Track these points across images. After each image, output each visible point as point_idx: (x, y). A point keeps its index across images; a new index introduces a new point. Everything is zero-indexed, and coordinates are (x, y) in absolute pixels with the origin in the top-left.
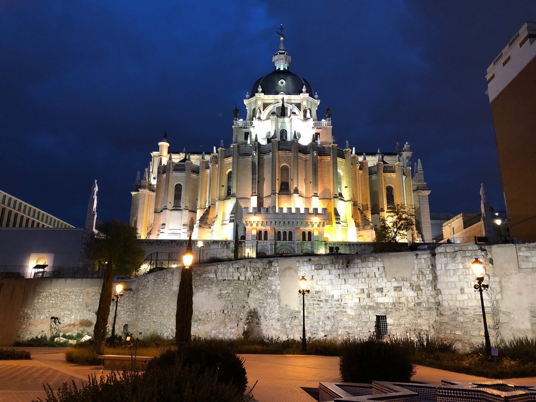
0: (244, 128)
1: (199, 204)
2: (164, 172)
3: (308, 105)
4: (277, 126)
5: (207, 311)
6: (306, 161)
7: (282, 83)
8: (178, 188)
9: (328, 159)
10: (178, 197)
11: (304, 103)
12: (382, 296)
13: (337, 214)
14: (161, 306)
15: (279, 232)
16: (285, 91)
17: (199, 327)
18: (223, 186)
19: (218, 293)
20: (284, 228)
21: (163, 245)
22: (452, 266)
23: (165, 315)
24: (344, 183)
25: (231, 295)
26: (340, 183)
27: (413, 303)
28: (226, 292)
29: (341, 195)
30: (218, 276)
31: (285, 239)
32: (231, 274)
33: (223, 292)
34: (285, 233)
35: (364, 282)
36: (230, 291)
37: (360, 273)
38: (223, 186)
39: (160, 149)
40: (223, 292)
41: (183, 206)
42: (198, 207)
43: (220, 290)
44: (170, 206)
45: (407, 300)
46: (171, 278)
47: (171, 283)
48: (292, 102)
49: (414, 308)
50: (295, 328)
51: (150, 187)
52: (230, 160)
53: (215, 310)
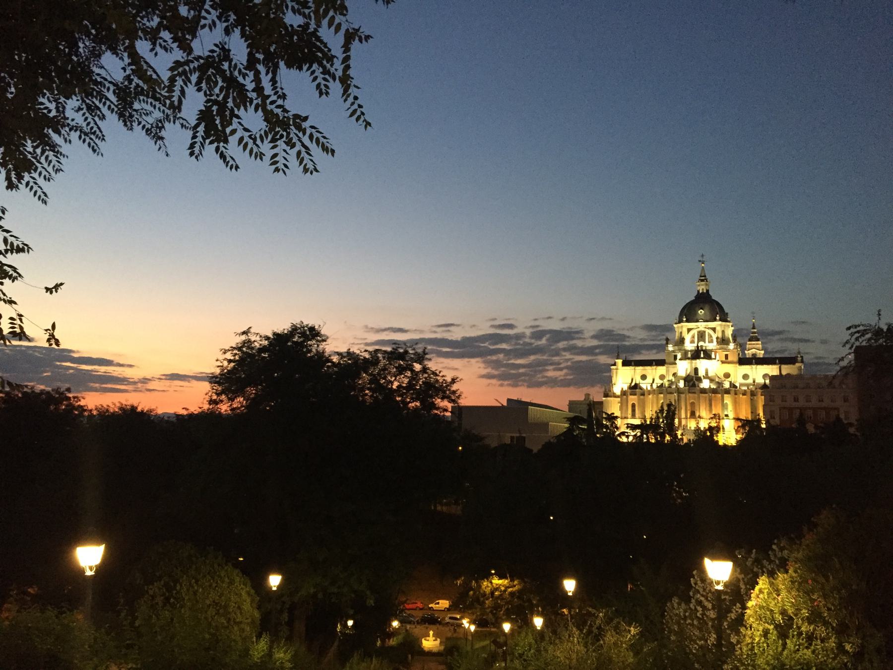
0: (674, 352)
2: (625, 395)
3: (721, 327)
4: (691, 366)
6: (706, 397)
7: (701, 312)
8: (633, 406)
9: (720, 395)
10: (633, 411)
11: (719, 329)
13: (723, 428)
15: (690, 439)
16: (703, 318)
24: (730, 407)
26: (727, 409)
29: (727, 416)
39: (617, 365)
41: (637, 416)
44: (630, 416)
48: (709, 327)
51: (615, 396)
52: (662, 395)
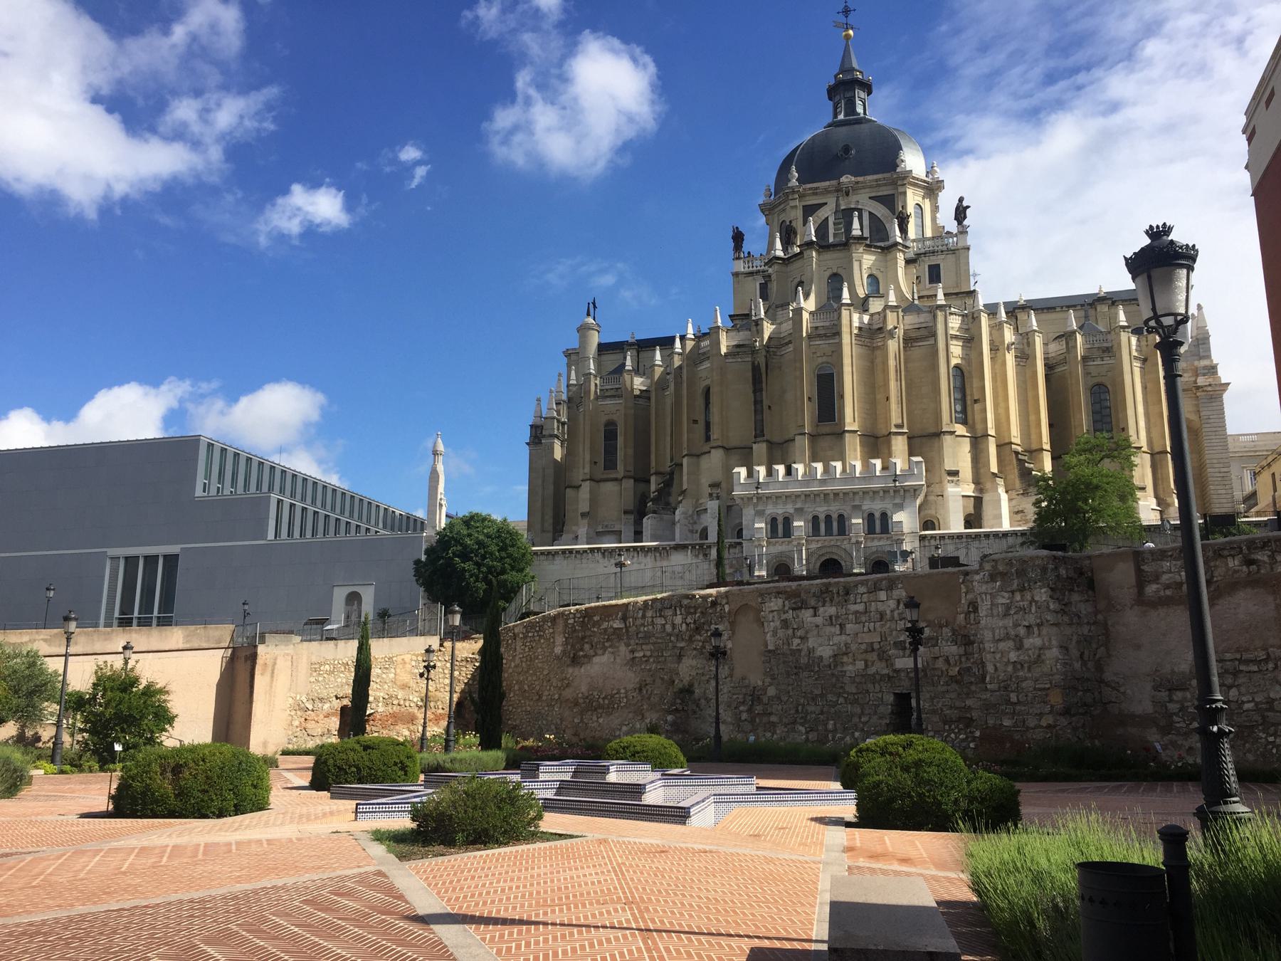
1: (653, 464)
5: (613, 690)
12: (904, 656)
14: (537, 683)
17: (601, 720)
18: (695, 422)
19: (629, 656)
20: (826, 508)
21: (575, 557)
22: (1004, 597)
23: (544, 698)
25: (651, 660)
27: (957, 669)
28: (641, 654)
30: (628, 624)
31: (829, 532)
32: (650, 620)
33: (637, 655)
34: (828, 518)
35: (872, 629)
36: (648, 653)
37: (866, 612)
38: (695, 422)
40: (637, 655)
42: (652, 471)
43: (632, 651)
45: (947, 661)
46: (551, 630)
47: (552, 640)
49: (959, 678)
50: (757, 720)
53: (625, 688)
